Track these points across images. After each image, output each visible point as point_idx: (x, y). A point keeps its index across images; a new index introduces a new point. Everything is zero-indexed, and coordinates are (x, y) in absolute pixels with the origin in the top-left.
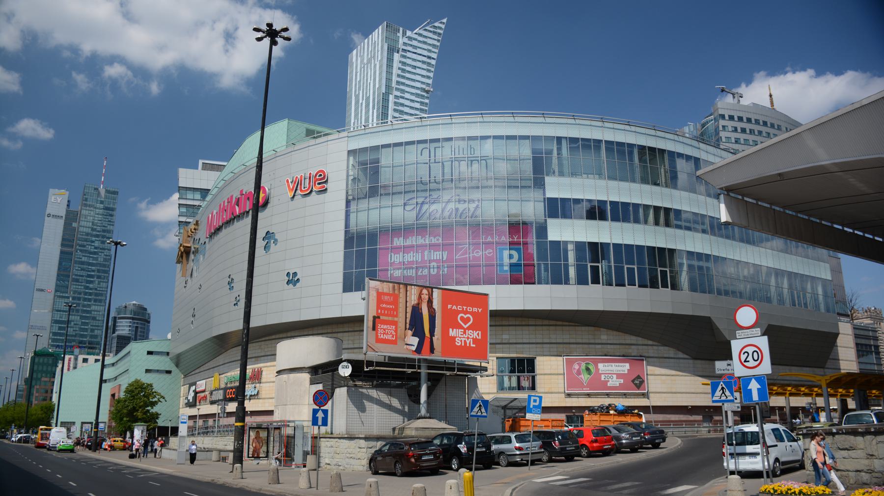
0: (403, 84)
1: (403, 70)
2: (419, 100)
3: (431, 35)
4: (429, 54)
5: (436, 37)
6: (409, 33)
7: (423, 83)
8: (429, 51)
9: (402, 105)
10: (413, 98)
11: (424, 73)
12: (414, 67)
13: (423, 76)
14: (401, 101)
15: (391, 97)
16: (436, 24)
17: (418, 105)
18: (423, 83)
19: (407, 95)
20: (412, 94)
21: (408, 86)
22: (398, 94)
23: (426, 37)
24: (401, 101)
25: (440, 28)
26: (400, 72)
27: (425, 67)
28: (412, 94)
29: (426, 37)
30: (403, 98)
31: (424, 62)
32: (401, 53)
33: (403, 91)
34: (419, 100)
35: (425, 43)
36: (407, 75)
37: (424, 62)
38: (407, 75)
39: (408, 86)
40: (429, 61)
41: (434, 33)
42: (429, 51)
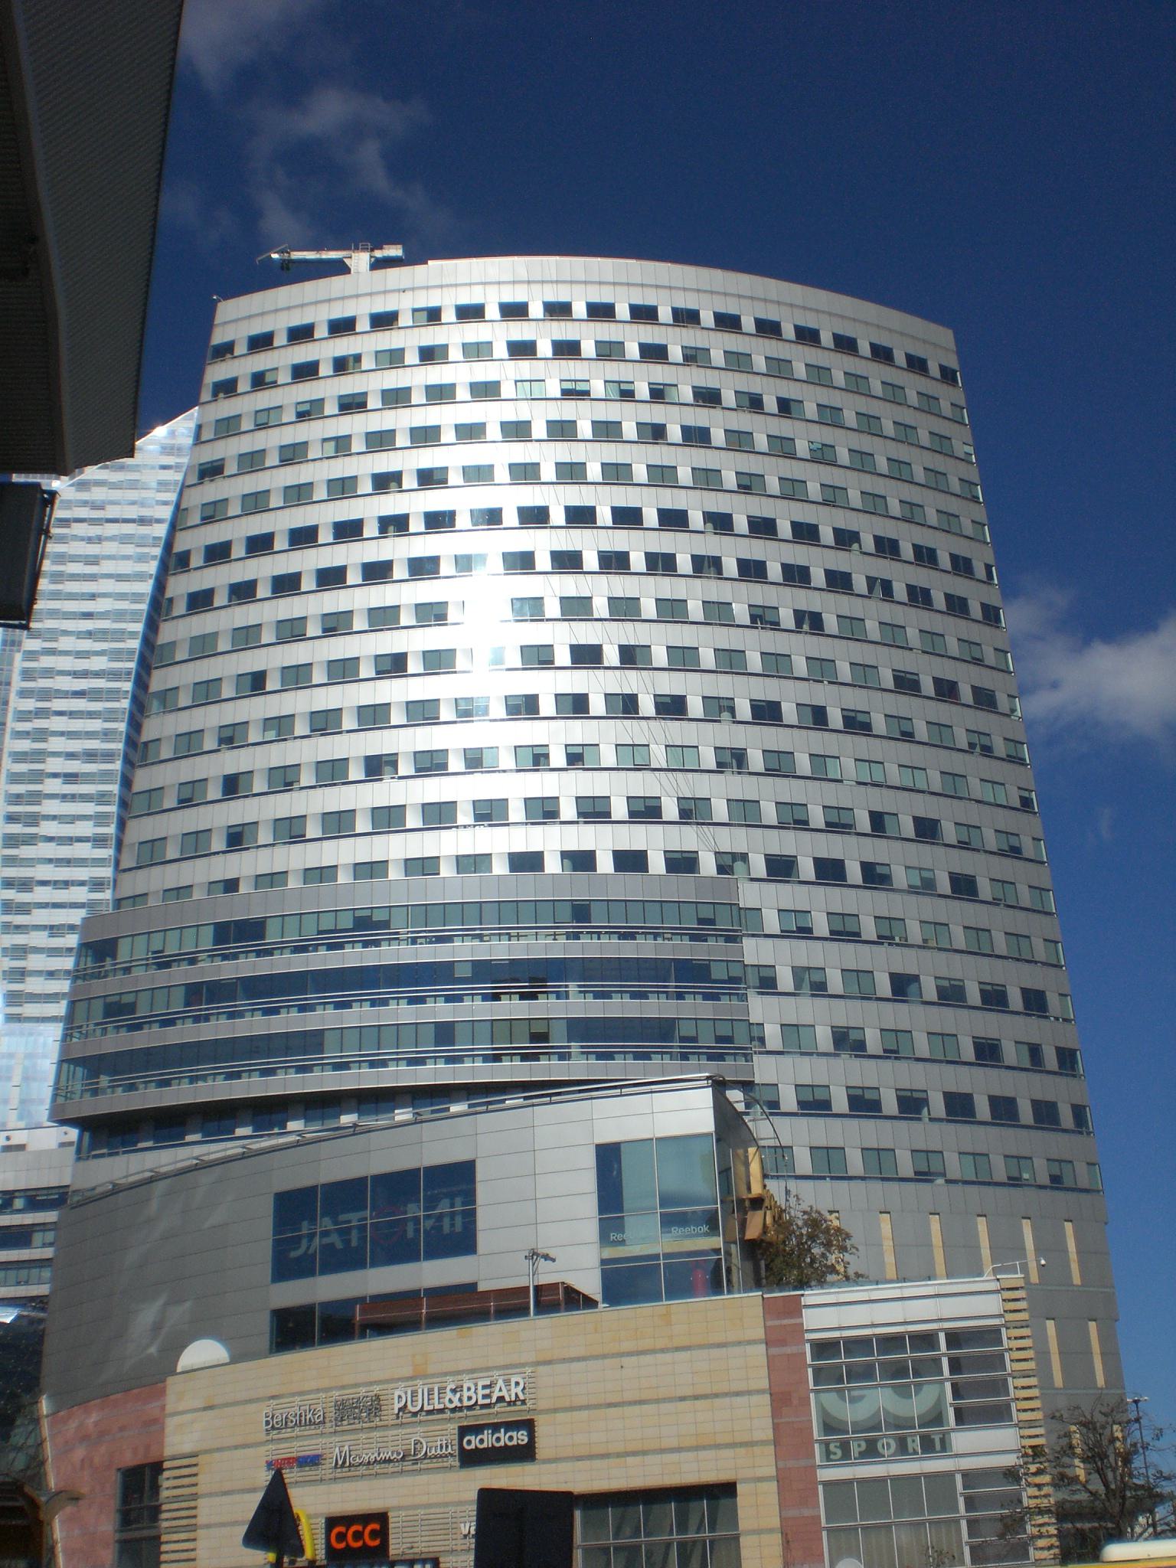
2: (104, 646)
9: (49, 673)
10: (86, 645)
12: (94, 560)
13: (120, 578)
14: (46, 662)
17: (99, 663)
19: (65, 643)
24: (46, 662)
27: (130, 550)
30: (52, 652)
31: (125, 539)
34: (104, 646)
37: (125, 539)
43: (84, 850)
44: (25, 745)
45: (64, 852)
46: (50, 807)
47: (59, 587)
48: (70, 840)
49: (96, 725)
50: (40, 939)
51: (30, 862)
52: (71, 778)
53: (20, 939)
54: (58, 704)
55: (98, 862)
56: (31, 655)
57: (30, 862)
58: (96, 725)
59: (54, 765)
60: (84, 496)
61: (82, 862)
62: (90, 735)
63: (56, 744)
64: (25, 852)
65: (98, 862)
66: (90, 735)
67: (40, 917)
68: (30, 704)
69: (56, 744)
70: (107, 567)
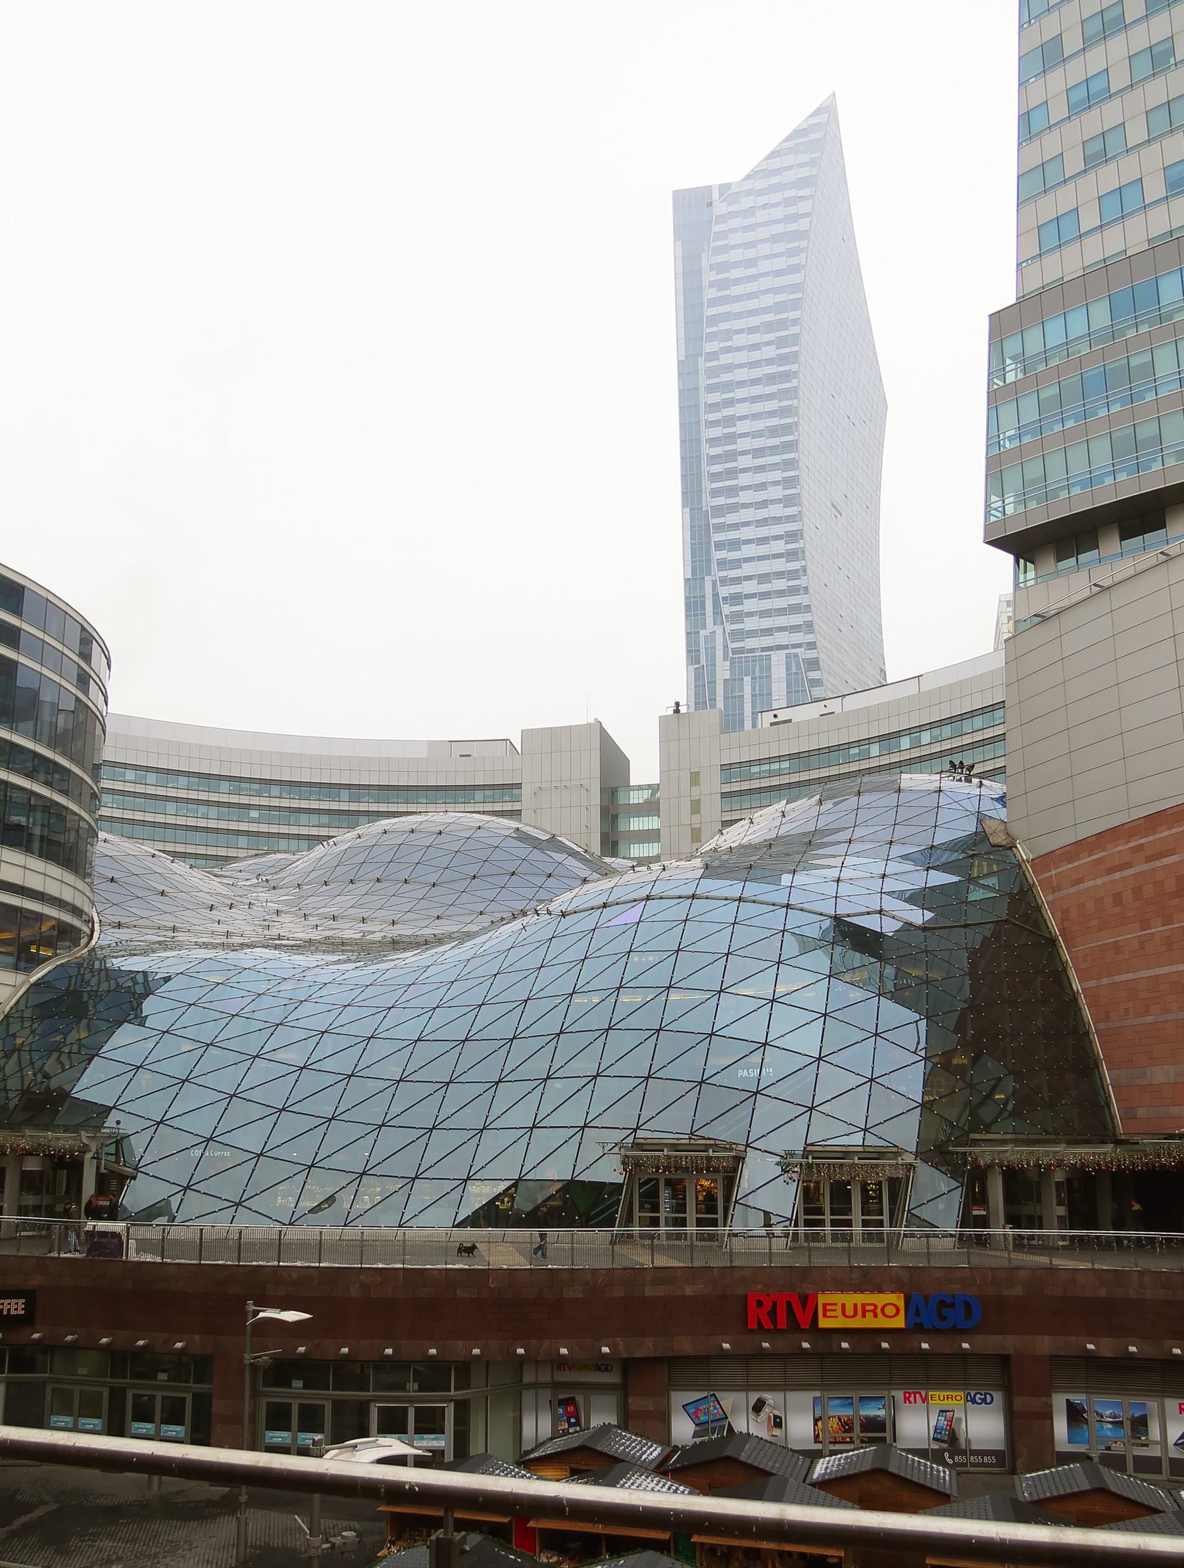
0: (727, 317)
2: (771, 337)
4: (791, 210)
8: (789, 202)
9: (729, 368)
10: (755, 338)
11: (780, 263)
13: (778, 273)
20: (752, 330)
21: (739, 316)
24: (725, 359)
27: (781, 247)
28: (752, 330)
30: (728, 350)
34: (771, 337)
37: (775, 239)
38: (736, 290)
39: (739, 316)
42: (789, 202)
44: (717, 432)
45: (762, 514)
46: (744, 479)
47: (727, 292)
48: (764, 504)
50: (750, 587)
51: (735, 527)
52: (758, 452)
53: (735, 589)
54: (740, 393)
56: (713, 356)
57: (735, 527)
59: (743, 444)
61: (777, 520)
62: (772, 414)
63: (742, 427)
64: (731, 518)
67: (748, 569)
68: (715, 398)
69: (742, 427)
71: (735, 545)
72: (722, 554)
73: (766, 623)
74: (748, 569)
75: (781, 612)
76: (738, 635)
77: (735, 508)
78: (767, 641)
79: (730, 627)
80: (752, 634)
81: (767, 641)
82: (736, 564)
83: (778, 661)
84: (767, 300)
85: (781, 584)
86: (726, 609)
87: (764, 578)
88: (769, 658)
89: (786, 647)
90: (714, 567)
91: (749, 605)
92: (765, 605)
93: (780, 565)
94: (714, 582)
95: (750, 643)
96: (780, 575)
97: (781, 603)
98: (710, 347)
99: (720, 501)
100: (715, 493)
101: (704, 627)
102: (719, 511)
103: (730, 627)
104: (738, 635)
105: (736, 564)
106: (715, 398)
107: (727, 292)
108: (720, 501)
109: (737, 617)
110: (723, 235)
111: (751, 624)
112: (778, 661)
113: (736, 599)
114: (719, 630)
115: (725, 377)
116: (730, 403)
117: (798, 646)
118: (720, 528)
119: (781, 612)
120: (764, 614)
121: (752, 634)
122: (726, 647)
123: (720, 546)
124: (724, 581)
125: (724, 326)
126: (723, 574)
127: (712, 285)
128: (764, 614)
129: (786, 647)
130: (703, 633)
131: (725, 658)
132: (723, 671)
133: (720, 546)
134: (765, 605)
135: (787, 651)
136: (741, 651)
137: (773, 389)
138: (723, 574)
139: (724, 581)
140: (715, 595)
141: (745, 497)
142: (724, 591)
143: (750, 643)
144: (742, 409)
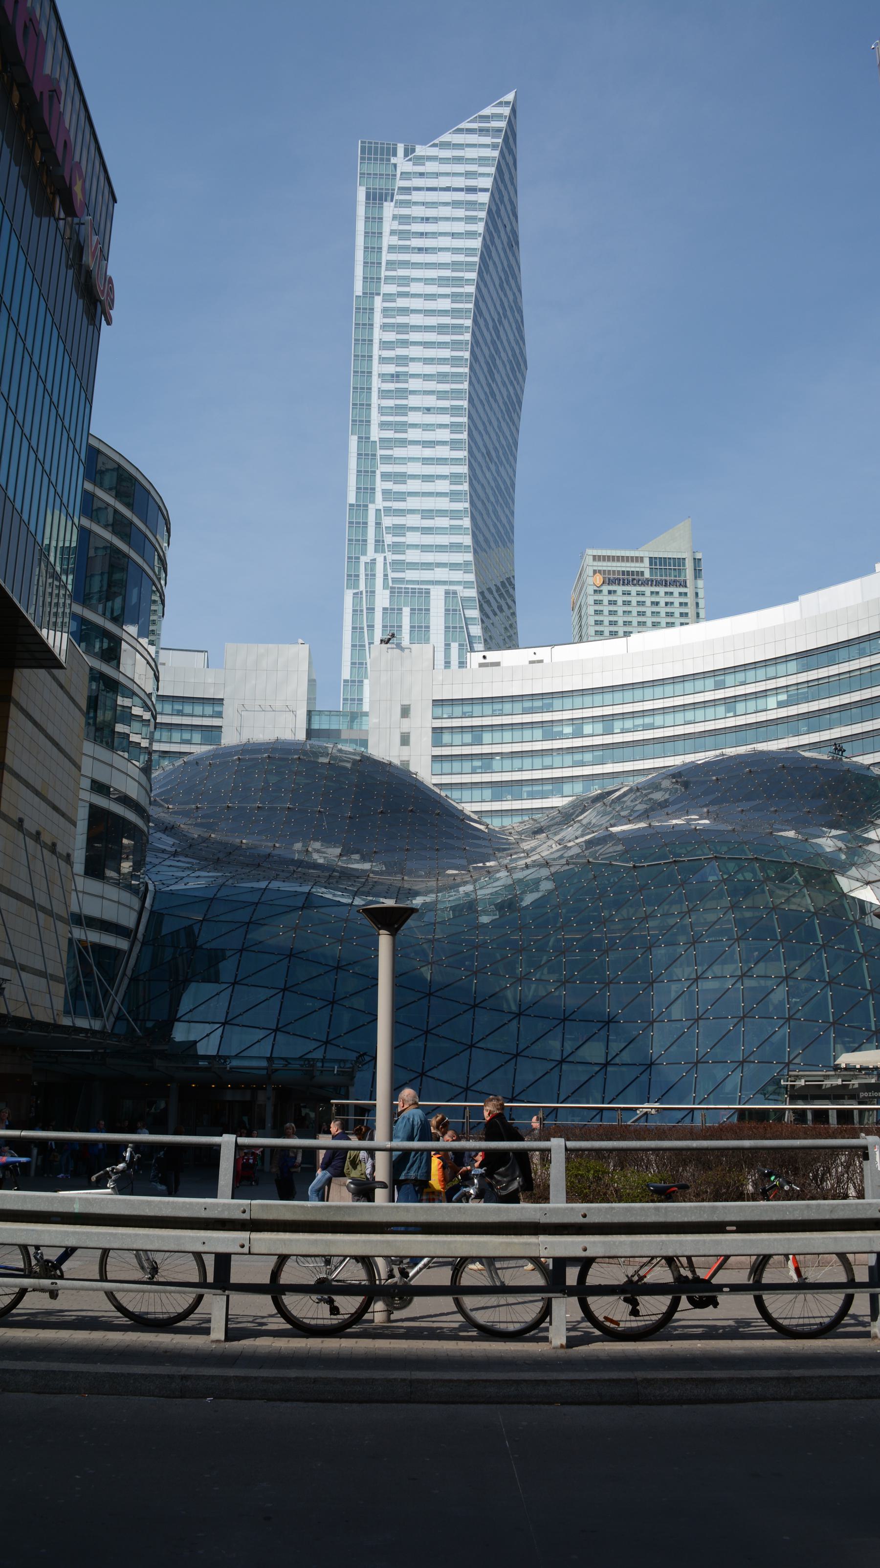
1: (404, 235)
3: (473, 139)
4: (471, 183)
5: (487, 140)
6: (420, 150)
7: (456, 251)
8: (468, 175)
9: (405, 311)
11: (460, 227)
14: (402, 303)
15: (378, 302)
16: (487, 111)
17: (445, 304)
18: (456, 251)
20: (427, 281)
22: (391, 289)
23: (460, 146)
24: (402, 303)
25: (499, 117)
26: (395, 241)
27: (461, 213)
28: (427, 281)
29: (460, 146)
31: (456, 204)
32: (396, 197)
33: (406, 281)
35: (458, 160)
36: (416, 242)
37: (456, 204)
40: (471, 197)
41: (482, 131)
42: (468, 175)
43: (443, 452)
45: (428, 453)
47: (407, 243)
49: (446, 353)
50: (413, 520)
51: (403, 460)
55: (455, 461)
56: (388, 297)
57: (403, 460)
58: (446, 353)
60: (420, 169)
62: (442, 361)
64: (398, 452)
65: (455, 461)
66: (442, 361)
67: (412, 503)
68: (391, 336)
70: (444, 227)
71: (401, 478)
72: (389, 485)
73: (429, 557)
74: (412, 503)
75: (441, 548)
76: (398, 566)
77: (404, 443)
78: (427, 575)
79: (391, 557)
80: (413, 566)
81: (427, 575)
82: (401, 496)
83: (437, 595)
84: (446, 258)
85: (443, 522)
86: (389, 539)
87: (427, 514)
88: (428, 592)
89: (444, 583)
90: (379, 496)
91: (412, 538)
92: (428, 540)
93: (444, 504)
94: (378, 511)
95: (410, 575)
96: (442, 513)
97: (444, 540)
98: (386, 289)
99: (389, 434)
100: (383, 425)
101: (364, 553)
102: (386, 443)
103: (391, 557)
104: (398, 566)
105: (401, 496)
106: (391, 336)
107: (407, 243)
108: (389, 434)
109: (397, 548)
110: (407, 190)
111: (412, 556)
112: (437, 595)
113: (399, 530)
114: (380, 558)
115: (401, 320)
116: (405, 343)
117: (458, 583)
118: (387, 459)
119: (441, 548)
120: (425, 548)
121: (413, 566)
122: (386, 575)
123: (386, 476)
124: (388, 511)
125: (401, 272)
126: (388, 504)
127: (393, 233)
128: (425, 548)
129: (444, 583)
130: (363, 559)
131: (385, 587)
132: (382, 599)
133: (386, 476)
134: (428, 540)
135: (447, 587)
136: (401, 581)
137: (447, 338)
138: (388, 504)
139: (388, 511)
140: (378, 524)
141: (413, 434)
142: (387, 521)
143: (410, 575)
144: (414, 352)
